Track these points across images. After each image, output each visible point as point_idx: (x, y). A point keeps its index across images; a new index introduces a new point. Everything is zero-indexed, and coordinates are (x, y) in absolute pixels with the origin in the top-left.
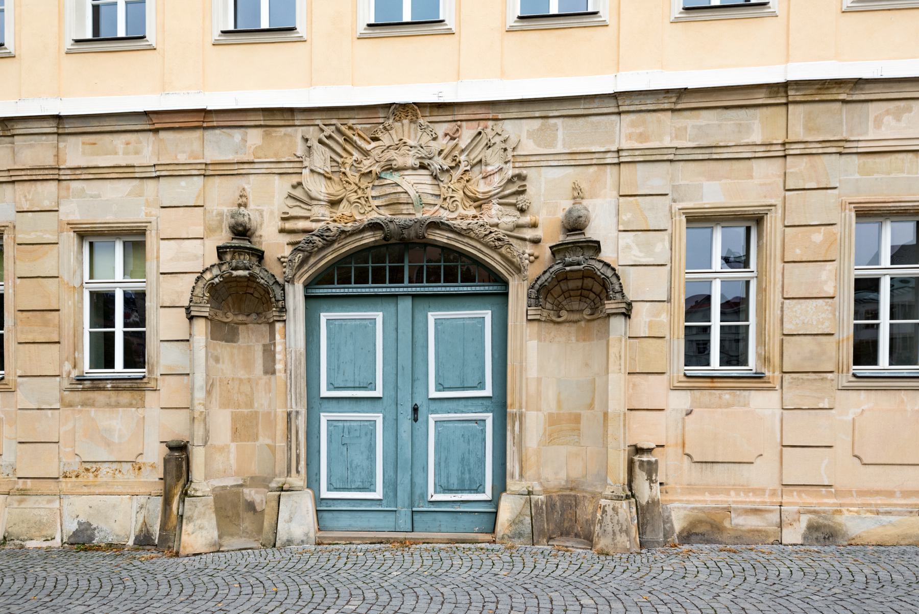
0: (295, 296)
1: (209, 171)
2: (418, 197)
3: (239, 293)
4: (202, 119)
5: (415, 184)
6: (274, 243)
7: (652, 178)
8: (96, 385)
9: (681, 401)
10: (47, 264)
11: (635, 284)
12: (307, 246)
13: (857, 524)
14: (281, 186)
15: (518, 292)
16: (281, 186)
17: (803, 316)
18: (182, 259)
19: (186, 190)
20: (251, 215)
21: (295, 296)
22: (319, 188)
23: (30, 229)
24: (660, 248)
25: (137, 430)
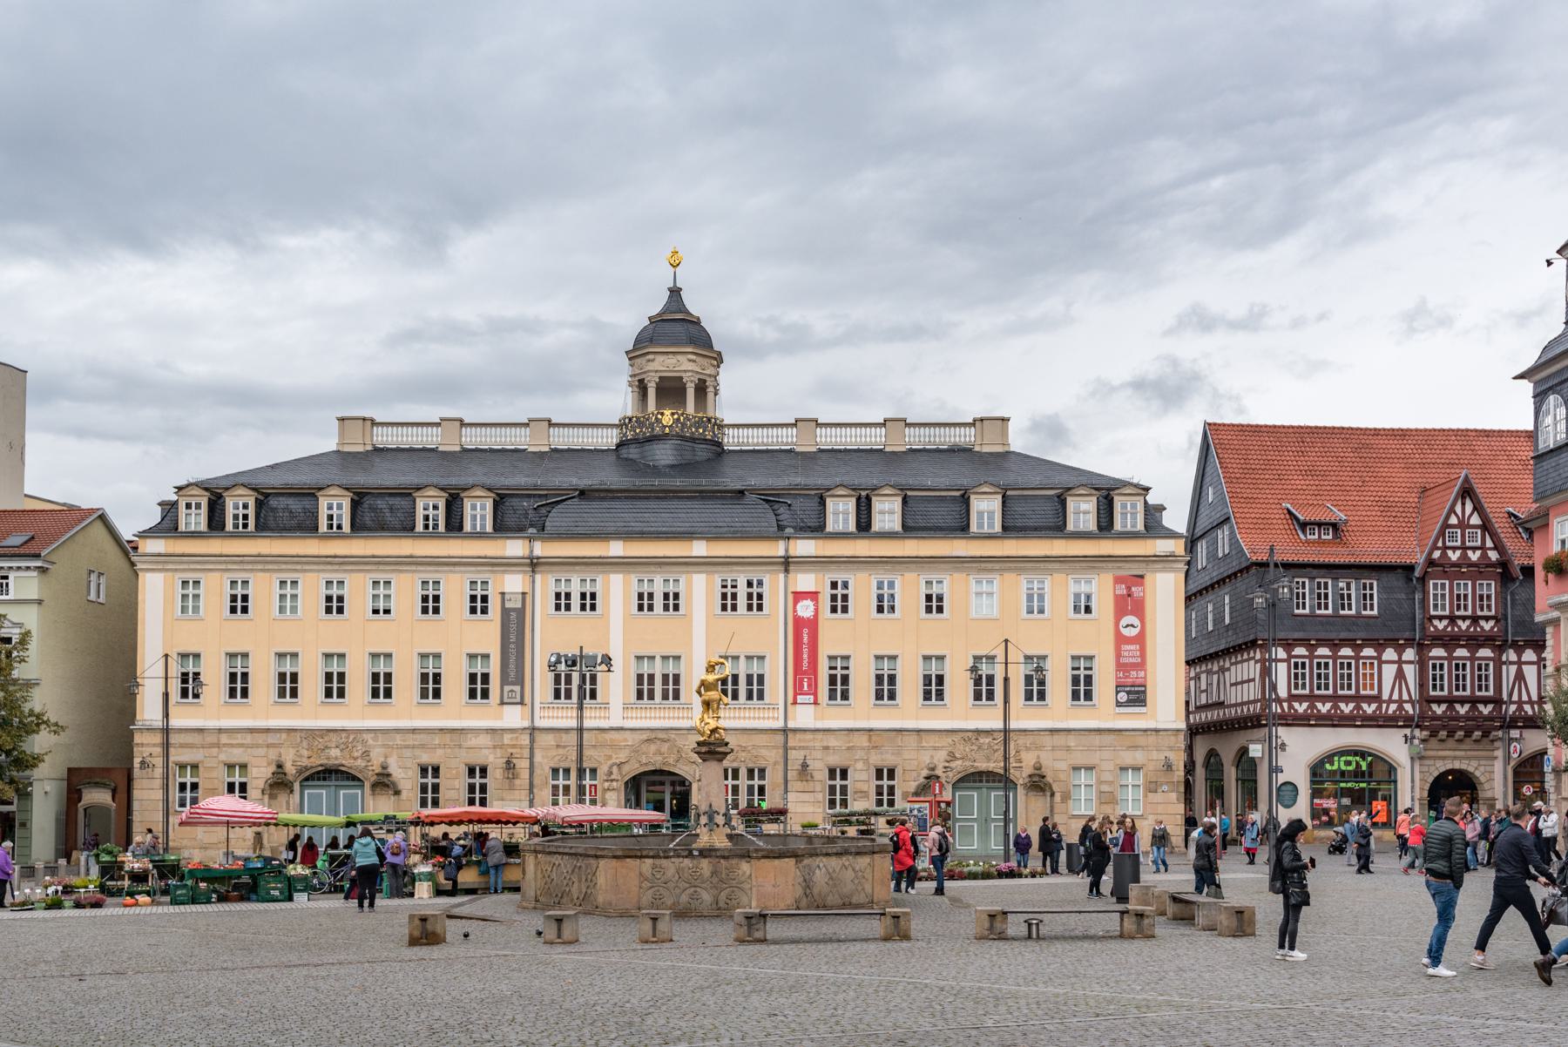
0: (297, 786)
1: (268, 746)
2: (335, 756)
3: (279, 783)
4: (268, 730)
5: (335, 752)
6: (290, 769)
7: (408, 753)
10: (214, 774)
12: (300, 772)
14: (292, 751)
15: (367, 785)
16: (292, 751)
17: (452, 794)
18: (260, 775)
19: (262, 751)
21: (297, 786)
22: (305, 753)
23: (210, 763)
24: (410, 773)
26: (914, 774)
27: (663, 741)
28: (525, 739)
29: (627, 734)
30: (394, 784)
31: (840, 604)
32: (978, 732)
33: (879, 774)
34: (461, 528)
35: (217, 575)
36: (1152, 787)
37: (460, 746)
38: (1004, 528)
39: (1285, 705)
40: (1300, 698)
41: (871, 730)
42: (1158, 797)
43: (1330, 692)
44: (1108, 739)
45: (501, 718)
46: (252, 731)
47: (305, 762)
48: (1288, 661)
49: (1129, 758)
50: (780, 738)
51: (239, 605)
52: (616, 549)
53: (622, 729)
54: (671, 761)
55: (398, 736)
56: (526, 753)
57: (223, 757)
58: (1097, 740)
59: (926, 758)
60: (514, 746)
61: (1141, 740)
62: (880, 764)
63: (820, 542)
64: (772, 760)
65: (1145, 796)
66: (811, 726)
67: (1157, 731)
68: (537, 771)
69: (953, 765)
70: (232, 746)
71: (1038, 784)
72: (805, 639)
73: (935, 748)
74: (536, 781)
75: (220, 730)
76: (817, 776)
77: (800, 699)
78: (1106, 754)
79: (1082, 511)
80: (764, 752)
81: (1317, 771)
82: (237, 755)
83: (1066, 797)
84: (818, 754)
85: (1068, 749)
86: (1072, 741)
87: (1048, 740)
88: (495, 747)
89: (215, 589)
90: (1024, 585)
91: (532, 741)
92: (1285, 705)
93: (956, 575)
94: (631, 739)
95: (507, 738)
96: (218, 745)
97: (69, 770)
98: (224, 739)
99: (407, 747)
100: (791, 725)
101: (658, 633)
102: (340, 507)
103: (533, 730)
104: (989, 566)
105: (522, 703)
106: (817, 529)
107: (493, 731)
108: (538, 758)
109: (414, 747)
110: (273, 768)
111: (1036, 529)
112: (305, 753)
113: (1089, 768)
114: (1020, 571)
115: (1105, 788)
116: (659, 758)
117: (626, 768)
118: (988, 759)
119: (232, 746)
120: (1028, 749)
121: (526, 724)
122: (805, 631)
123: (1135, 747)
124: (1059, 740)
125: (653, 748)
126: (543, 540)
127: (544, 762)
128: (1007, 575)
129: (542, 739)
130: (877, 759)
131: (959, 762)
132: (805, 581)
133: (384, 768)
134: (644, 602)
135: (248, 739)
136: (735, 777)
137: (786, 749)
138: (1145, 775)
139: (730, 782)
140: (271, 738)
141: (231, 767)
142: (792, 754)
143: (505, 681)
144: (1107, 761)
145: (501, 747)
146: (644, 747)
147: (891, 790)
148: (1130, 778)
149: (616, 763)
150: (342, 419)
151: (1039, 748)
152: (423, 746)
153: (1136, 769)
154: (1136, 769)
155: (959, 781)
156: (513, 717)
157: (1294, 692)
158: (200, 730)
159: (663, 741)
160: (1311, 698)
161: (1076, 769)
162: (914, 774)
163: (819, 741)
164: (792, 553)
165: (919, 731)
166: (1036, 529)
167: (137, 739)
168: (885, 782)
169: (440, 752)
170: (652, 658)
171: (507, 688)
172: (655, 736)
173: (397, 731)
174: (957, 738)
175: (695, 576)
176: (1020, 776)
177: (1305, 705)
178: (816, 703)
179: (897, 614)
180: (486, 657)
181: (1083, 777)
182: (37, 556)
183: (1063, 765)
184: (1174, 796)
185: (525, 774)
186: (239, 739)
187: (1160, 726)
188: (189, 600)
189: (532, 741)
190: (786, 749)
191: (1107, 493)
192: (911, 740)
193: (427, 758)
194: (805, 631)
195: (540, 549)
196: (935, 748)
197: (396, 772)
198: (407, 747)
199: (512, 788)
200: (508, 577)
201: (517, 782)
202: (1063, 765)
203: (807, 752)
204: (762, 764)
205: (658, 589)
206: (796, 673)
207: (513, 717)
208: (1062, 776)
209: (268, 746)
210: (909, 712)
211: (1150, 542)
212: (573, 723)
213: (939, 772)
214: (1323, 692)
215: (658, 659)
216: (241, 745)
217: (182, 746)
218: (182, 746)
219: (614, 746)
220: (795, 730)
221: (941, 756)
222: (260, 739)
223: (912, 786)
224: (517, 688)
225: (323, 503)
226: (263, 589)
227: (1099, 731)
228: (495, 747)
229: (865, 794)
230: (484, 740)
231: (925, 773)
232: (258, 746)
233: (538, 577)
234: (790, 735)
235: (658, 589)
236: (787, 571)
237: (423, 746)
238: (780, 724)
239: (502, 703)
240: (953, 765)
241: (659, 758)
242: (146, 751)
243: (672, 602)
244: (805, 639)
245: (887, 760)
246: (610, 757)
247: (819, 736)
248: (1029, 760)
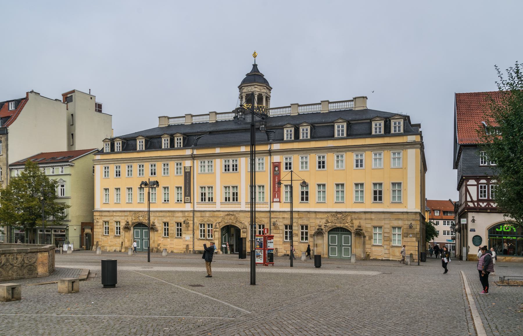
1: (125, 216)
3: (127, 228)
4: (124, 211)
5: (141, 218)
6: (130, 223)
7: (160, 218)
8: (116, 236)
9: (162, 239)
11: (159, 228)
12: (133, 223)
13: (175, 251)
18: (123, 224)
19: (123, 218)
20: (128, 221)
21: (132, 228)
22: (134, 218)
25: (119, 241)
26: (314, 228)
27: (232, 215)
28: (191, 214)
29: (221, 213)
30: (156, 228)
31: (288, 166)
32: (337, 213)
33: (302, 228)
34: (174, 147)
35: (112, 165)
36: (405, 235)
37: (174, 216)
38: (348, 135)
39: (476, 204)
40: (483, 201)
41: (299, 212)
42: (408, 239)
43: (486, 198)
44: (387, 216)
45: (185, 207)
46: (121, 211)
47: (134, 221)
48: (477, 185)
49: (396, 223)
50: (268, 214)
51: (118, 174)
52: (218, 150)
53: (219, 211)
55: (157, 213)
56: (192, 219)
57: (114, 219)
58: (383, 216)
59: (318, 222)
60: (188, 217)
61: (401, 216)
62: (302, 224)
63: (282, 144)
64: (266, 222)
65: (403, 238)
66: (278, 210)
67: (407, 213)
68: (195, 225)
69: (328, 224)
70: (116, 216)
71: (359, 233)
72: (277, 180)
73: (321, 218)
74: (195, 228)
75: (113, 211)
76: (281, 228)
77: (275, 200)
78: (387, 222)
79: (377, 126)
80: (263, 219)
81: (492, 231)
82: (118, 219)
83: (371, 238)
84: (281, 220)
85: (371, 219)
86: (373, 216)
87: (363, 216)
88: (183, 217)
89: (113, 169)
90: (355, 158)
91: (194, 215)
92: (476, 204)
93: (329, 154)
94: (222, 214)
95: (186, 214)
96: (112, 216)
97: (82, 223)
98: (114, 214)
99: (160, 217)
100: (272, 210)
101: (231, 179)
102: (142, 142)
103: (194, 211)
104: (341, 150)
105: (190, 202)
106: (281, 140)
107: (182, 211)
108: (195, 221)
109: (161, 217)
110: (126, 223)
111: (360, 135)
112: (134, 218)
113: (380, 227)
114: (353, 151)
115: (386, 235)
116: (231, 221)
117: (221, 224)
118: (341, 223)
119: (116, 216)
120: (356, 219)
121: (192, 209)
122: (277, 177)
123: (399, 219)
124: (368, 216)
125: (229, 217)
126: (197, 149)
127: (197, 221)
128: (348, 153)
129: (198, 214)
130: (301, 222)
131: (330, 224)
132: (276, 158)
133: (154, 223)
134: (227, 168)
135: (120, 214)
137: (270, 218)
138: (403, 230)
140: (126, 214)
141: (117, 222)
142: (273, 220)
143: (185, 196)
144: (387, 224)
145: (185, 217)
146: (226, 217)
147: (307, 233)
148: (397, 231)
149: (219, 222)
150: (159, 117)
151: (360, 219)
152: (164, 216)
153: (399, 228)
154: (399, 228)
155: (330, 231)
156: (188, 207)
157: (480, 198)
158: (109, 211)
159: (232, 215)
160: (488, 201)
161: (375, 227)
162: (314, 228)
163: (281, 215)
164: (272, 149)
165: (315, 212)
166: (360, 135)
167: (95, 214)
168: (304, 231)
169: (168, 218)
170: (229, 187)
171: (186, 198)
172: (230, 213)
173: (157, 211)
174: (329, 215)
175: (242, 158)
176: (353, 230)
177: (496, 204)
178: (280, 202)
179: (308, 169)
180: (181, 188)
181: (378, 231)
182: (68, 162)
183: (369, 226)
184: (414, 239)
185: (191, 226)
186: (118, 214)
187: (408, 211)
188: (106, 174)
189: (194, 215)
190: (270, 218)
191: (387, 119)
192: (313, 215)
193: (165, 220)
194: (277, 177)
195: (196, 152)
196: (321, 218)
197: (156, 224)
198: (160, 217)
199: (188, 230)
200: (186, 161)
201: (189, 228)
202: (369, 226)
203: (277, 219)
204: (263, 223)
205: (231, 163)
206: (273, 192)
207: (188, 207)
208: (369, 230)
209: (125, 216)
210: (311, 206)
211: (405, 137)
212: (146, 209)
213: (323, 227)
214: (483, 198)
215: (231, 188)
216: (118, 216)
217: (105, 216)
218: (105, 216)
219: (218, 217)
220: (273, 212)
221: (324, 221)
222: (123, 214)
223: (313, 232)
224: (189, 198)
225: (138, 141)
226: (124, 168)
227: (383, 213)
228: (183, 217)
229: (297, 235)
230: (180, 214)
231: (317, 227)
232: (122, 216)
233: (195, 161)
234: (272, 213)
235: (231, 163)
236: (271, 155)
237: (164, 216)
238: (268, 209)
239: (185, 203)
240: (328, 224)
241: (231, 221)
242: (97, 217)
243: (235, 168)
244: (277, 180)
245: (305, 222)
246: (216, 220)
247: (281, 214)
248: (356, 223)
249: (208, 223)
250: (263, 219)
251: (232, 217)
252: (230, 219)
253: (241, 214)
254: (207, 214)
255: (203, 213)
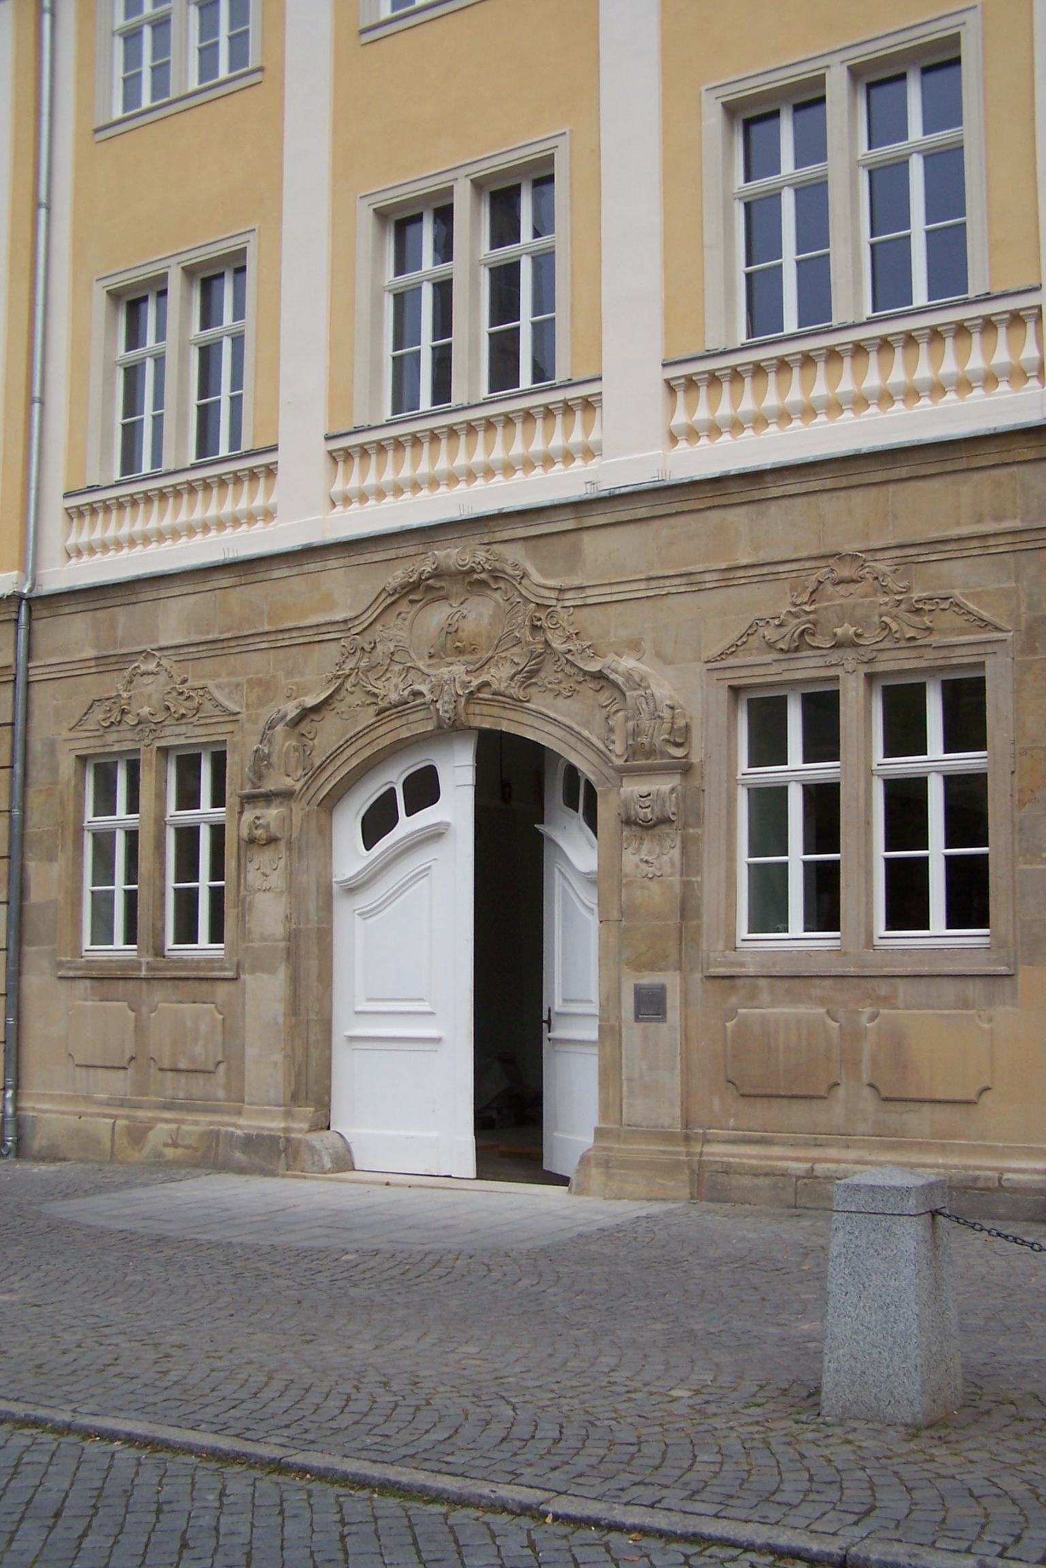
54: (499, 676)
94: (344, 593)
125: (436, 616)
136: (822, 743)
139: (796, 770)
146: (395, 631)
204: (955, 644)
249: (174, 737)
250: (958, 577)
251: (478, 614)
252: (453, 645)
253: (610, 552)
254: (173, 621)
255: (123, 617)
